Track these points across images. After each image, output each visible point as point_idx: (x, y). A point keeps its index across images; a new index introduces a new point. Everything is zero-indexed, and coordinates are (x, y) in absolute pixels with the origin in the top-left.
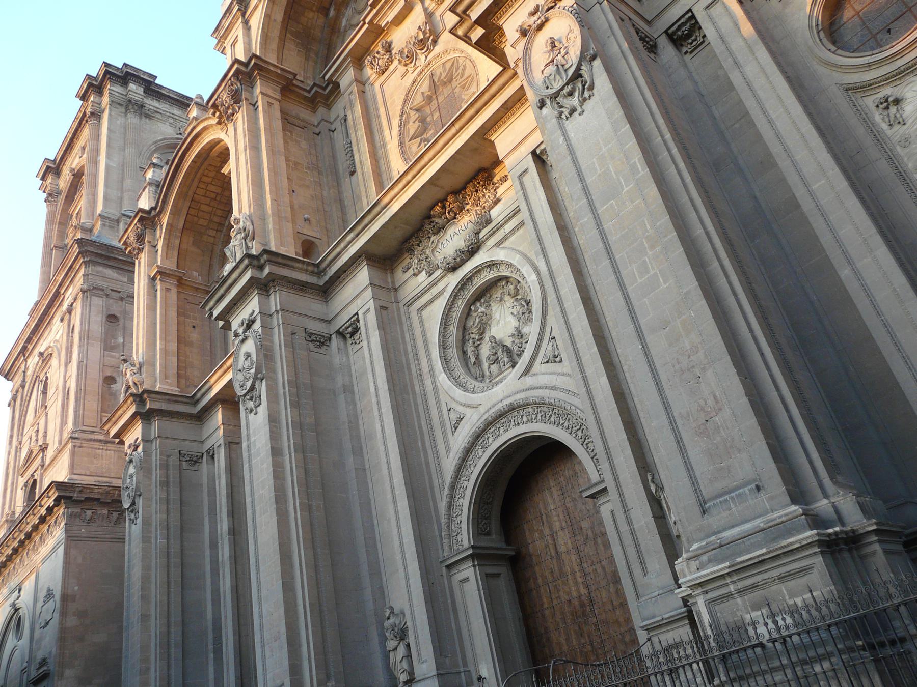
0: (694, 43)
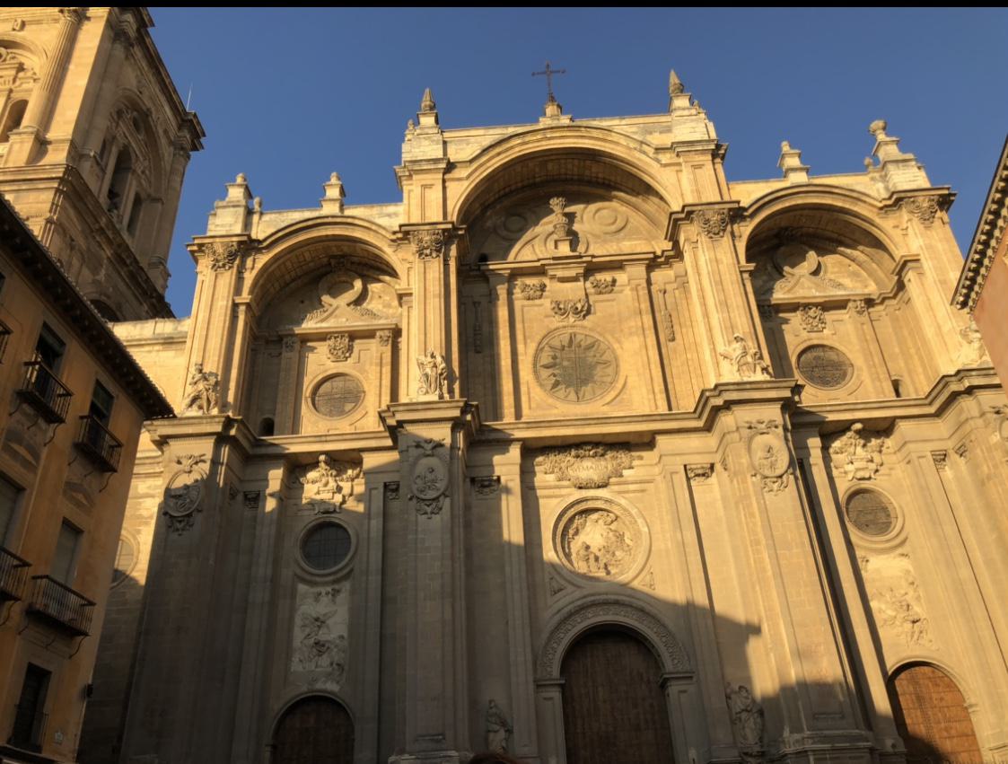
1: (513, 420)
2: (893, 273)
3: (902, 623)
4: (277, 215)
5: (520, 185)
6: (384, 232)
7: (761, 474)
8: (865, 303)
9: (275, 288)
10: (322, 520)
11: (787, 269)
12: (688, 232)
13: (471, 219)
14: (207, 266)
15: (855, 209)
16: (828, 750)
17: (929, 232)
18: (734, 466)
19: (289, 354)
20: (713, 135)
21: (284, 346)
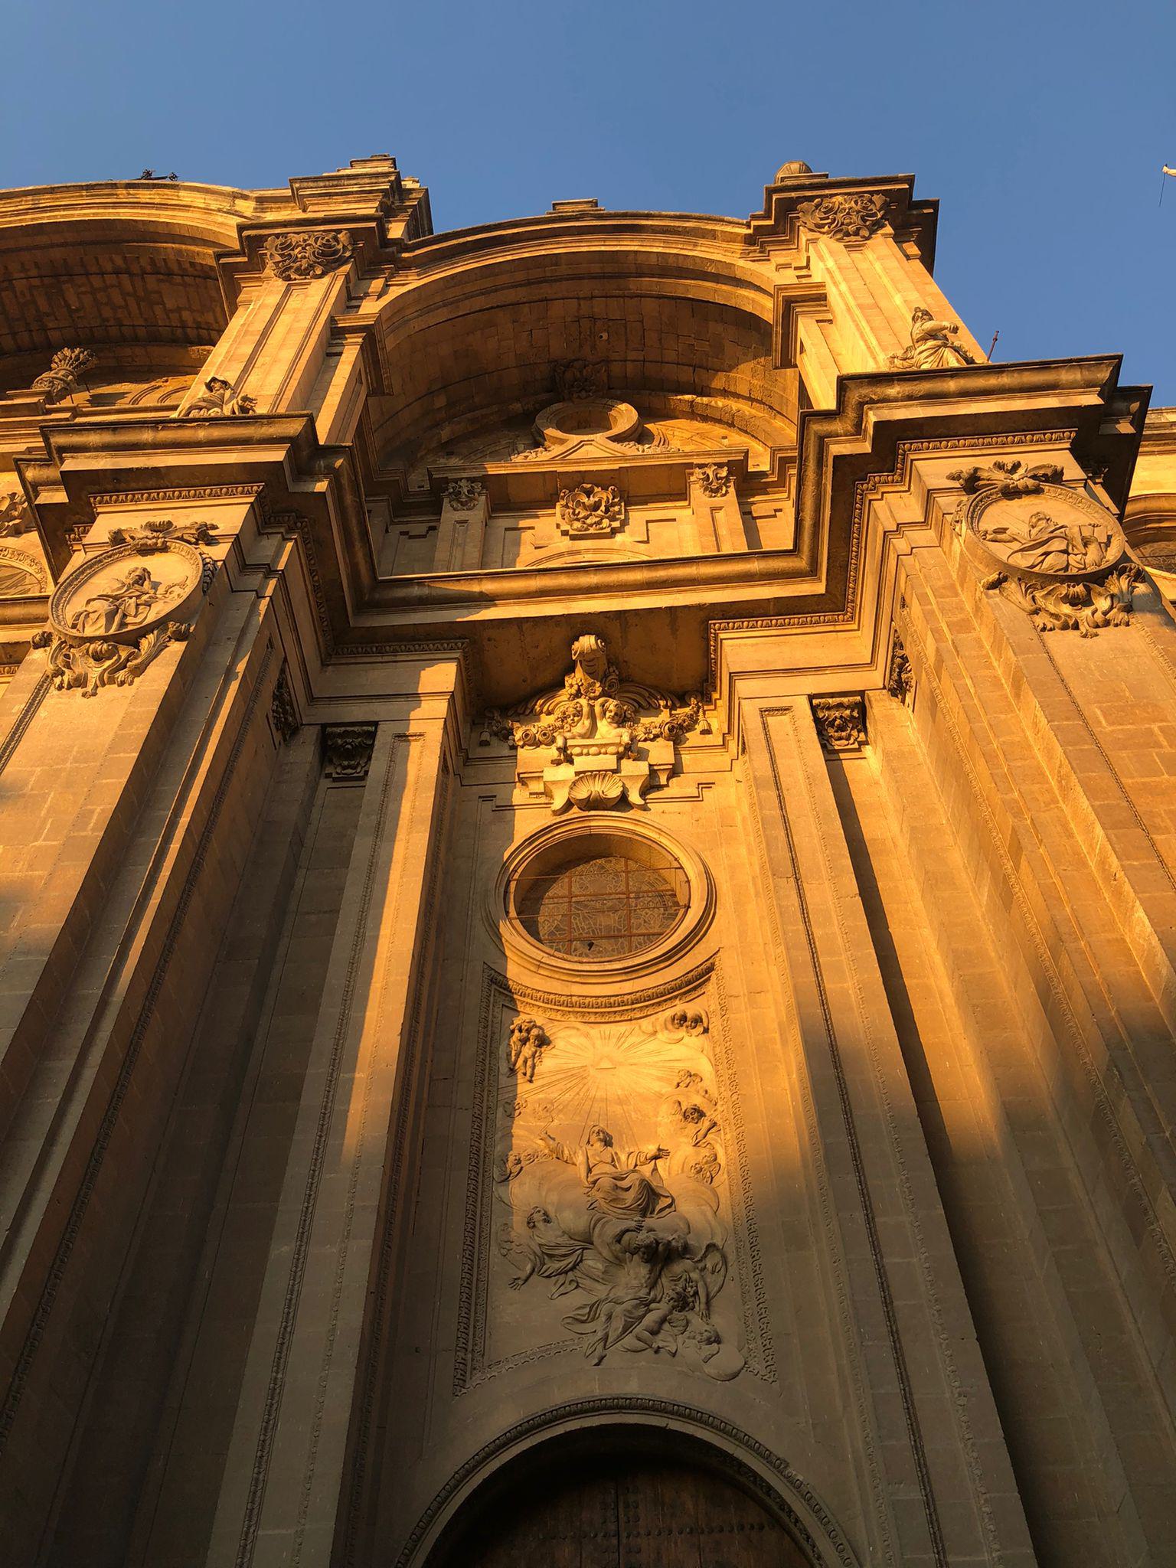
0: (350, 771)
8: (730, 473)
17: (856, 255)
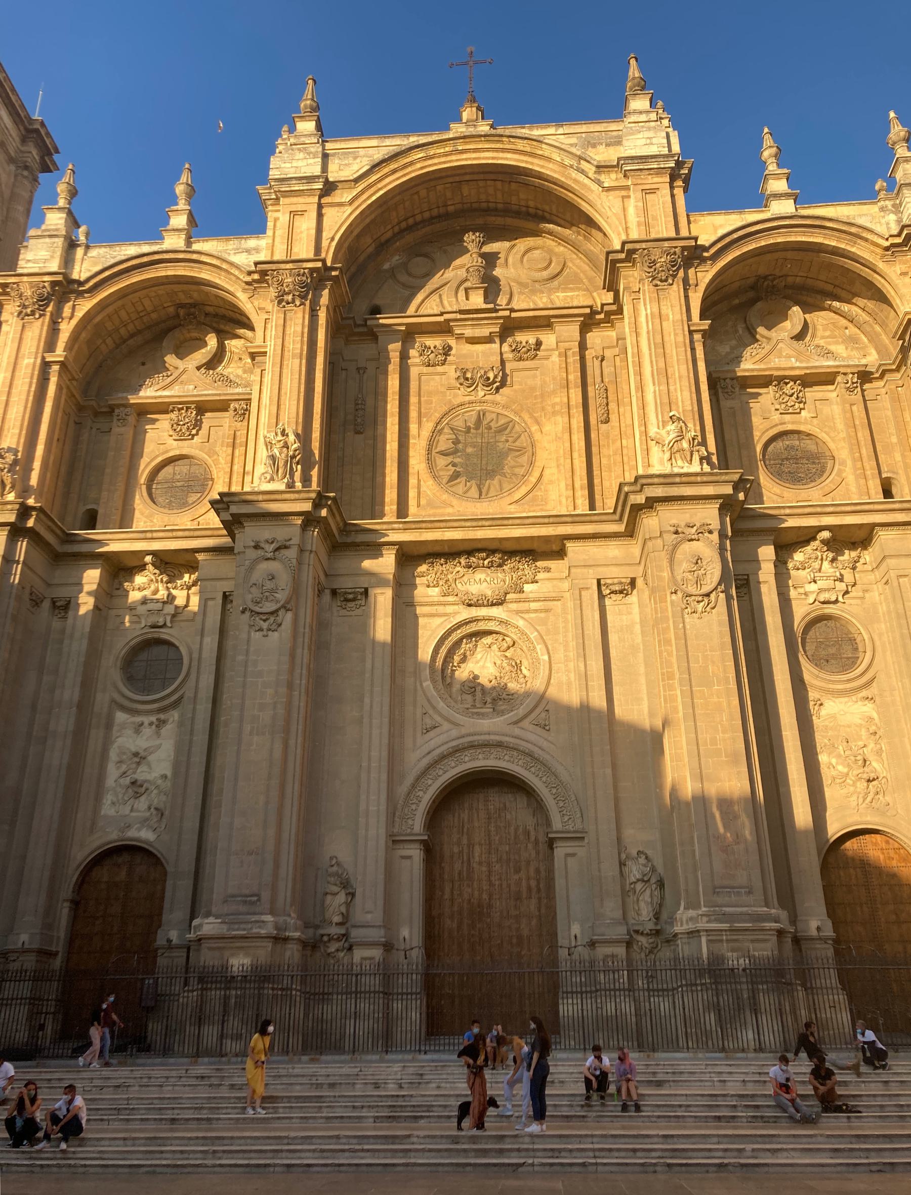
1: (394, 519)
2: (893, 337)
3: (854, 782)
4: (107, 250)
5: (427, 215)
6: (237, 273)
7: (682, 590)
9: (107, 345)
10: (150, 636)
11: (761, 330)
12: (631, 277)
13: (362, 258)
14: (12, 314)
15: (853, 250)
16: (726, 930)
18: (653, 582)
19: (122, 430)
20: (676, 148)
21: (115, 418)
